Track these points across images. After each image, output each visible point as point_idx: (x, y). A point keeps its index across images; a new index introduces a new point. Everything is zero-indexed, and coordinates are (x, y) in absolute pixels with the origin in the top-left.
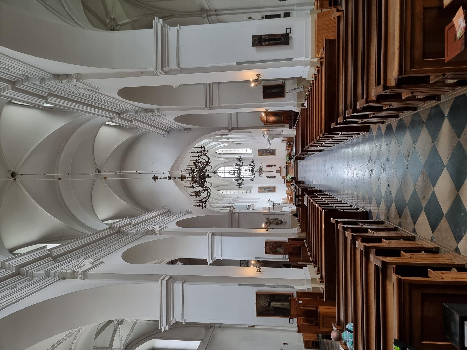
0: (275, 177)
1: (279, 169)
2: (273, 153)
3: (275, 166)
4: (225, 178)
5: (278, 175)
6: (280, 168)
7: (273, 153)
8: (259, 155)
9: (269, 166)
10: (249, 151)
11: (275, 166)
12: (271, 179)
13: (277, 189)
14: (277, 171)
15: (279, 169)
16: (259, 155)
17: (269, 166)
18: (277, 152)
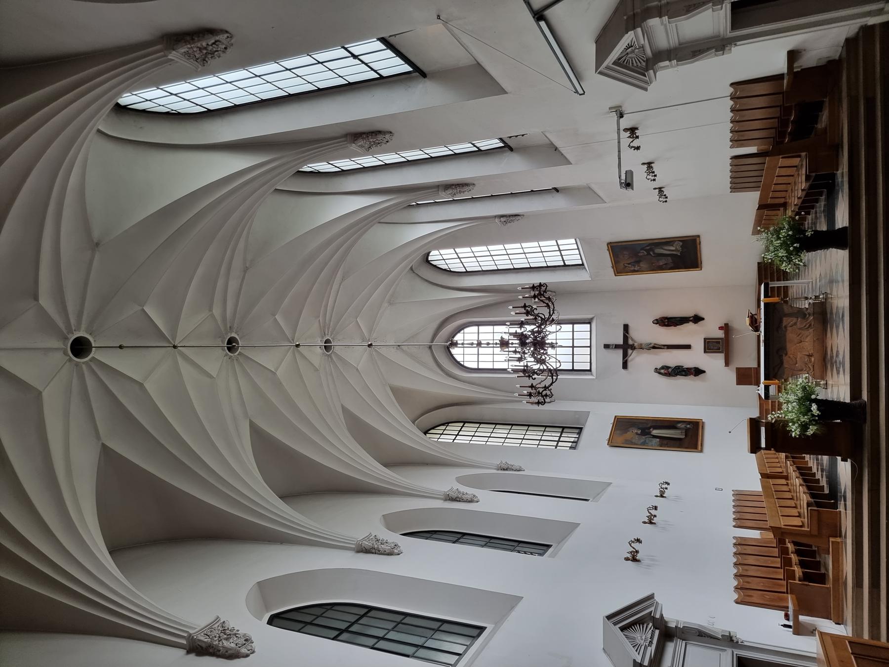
0: (698, 372)
1: (721, 334)
2: (684, 254)
3: (697, 319)
4: (478, 370)
5: (713, 363)
6: (726, 328)
7: (684, 254)
8: (618, 272)
9: (667, 322)
10: (573, 258)
11: (697, 319)
12: (681, 381)
13: (709, 437)
14: (711, 346)
15: (721, 334)
16: (618, 272)
17: (667, 322)
18: (706, 252)
